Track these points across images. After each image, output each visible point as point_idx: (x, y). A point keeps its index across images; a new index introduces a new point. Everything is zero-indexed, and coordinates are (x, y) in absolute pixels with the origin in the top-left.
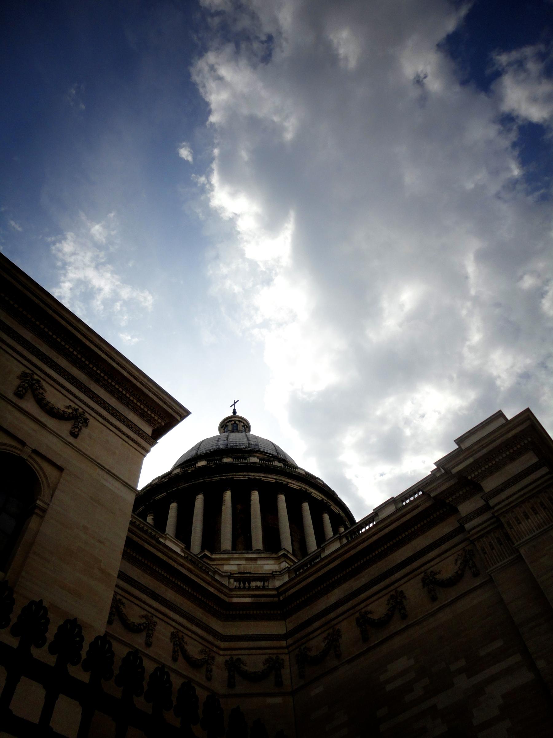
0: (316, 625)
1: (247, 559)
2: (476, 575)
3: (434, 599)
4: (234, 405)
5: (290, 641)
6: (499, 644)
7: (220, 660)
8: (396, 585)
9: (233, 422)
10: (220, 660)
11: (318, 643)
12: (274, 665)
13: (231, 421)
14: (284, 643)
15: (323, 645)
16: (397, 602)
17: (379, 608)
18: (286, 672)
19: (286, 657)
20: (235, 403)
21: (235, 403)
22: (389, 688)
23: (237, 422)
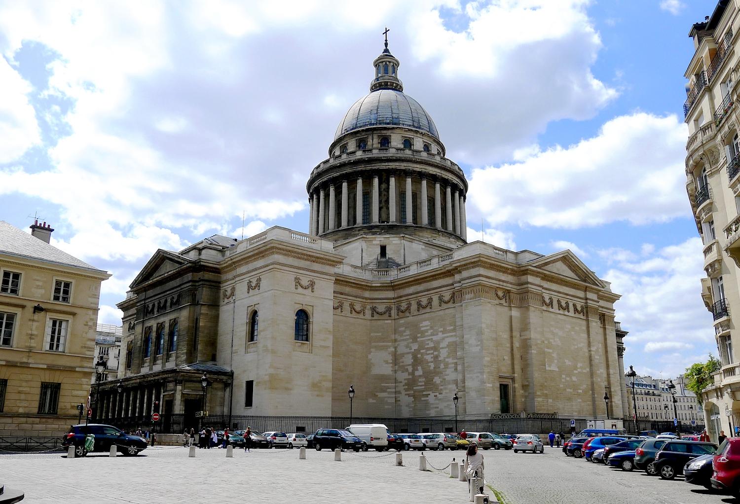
0: (404, 298)
1: (384, 238)
2: (454, 303)
4: (386, 33)
5: (395, 301)
6: (452, 327)
8: (431, 295)
9: (384, 63)
10: (368, 307)
11: (404, 306)
12: (389, 309)
13: (383, 62)
14: (393, 301)
16: (430, 301)
17: (424, 301)
19: (393, 306)
20: (386, 31)
21: (386, 31)
22: (422, 329)
23: (388, 63)
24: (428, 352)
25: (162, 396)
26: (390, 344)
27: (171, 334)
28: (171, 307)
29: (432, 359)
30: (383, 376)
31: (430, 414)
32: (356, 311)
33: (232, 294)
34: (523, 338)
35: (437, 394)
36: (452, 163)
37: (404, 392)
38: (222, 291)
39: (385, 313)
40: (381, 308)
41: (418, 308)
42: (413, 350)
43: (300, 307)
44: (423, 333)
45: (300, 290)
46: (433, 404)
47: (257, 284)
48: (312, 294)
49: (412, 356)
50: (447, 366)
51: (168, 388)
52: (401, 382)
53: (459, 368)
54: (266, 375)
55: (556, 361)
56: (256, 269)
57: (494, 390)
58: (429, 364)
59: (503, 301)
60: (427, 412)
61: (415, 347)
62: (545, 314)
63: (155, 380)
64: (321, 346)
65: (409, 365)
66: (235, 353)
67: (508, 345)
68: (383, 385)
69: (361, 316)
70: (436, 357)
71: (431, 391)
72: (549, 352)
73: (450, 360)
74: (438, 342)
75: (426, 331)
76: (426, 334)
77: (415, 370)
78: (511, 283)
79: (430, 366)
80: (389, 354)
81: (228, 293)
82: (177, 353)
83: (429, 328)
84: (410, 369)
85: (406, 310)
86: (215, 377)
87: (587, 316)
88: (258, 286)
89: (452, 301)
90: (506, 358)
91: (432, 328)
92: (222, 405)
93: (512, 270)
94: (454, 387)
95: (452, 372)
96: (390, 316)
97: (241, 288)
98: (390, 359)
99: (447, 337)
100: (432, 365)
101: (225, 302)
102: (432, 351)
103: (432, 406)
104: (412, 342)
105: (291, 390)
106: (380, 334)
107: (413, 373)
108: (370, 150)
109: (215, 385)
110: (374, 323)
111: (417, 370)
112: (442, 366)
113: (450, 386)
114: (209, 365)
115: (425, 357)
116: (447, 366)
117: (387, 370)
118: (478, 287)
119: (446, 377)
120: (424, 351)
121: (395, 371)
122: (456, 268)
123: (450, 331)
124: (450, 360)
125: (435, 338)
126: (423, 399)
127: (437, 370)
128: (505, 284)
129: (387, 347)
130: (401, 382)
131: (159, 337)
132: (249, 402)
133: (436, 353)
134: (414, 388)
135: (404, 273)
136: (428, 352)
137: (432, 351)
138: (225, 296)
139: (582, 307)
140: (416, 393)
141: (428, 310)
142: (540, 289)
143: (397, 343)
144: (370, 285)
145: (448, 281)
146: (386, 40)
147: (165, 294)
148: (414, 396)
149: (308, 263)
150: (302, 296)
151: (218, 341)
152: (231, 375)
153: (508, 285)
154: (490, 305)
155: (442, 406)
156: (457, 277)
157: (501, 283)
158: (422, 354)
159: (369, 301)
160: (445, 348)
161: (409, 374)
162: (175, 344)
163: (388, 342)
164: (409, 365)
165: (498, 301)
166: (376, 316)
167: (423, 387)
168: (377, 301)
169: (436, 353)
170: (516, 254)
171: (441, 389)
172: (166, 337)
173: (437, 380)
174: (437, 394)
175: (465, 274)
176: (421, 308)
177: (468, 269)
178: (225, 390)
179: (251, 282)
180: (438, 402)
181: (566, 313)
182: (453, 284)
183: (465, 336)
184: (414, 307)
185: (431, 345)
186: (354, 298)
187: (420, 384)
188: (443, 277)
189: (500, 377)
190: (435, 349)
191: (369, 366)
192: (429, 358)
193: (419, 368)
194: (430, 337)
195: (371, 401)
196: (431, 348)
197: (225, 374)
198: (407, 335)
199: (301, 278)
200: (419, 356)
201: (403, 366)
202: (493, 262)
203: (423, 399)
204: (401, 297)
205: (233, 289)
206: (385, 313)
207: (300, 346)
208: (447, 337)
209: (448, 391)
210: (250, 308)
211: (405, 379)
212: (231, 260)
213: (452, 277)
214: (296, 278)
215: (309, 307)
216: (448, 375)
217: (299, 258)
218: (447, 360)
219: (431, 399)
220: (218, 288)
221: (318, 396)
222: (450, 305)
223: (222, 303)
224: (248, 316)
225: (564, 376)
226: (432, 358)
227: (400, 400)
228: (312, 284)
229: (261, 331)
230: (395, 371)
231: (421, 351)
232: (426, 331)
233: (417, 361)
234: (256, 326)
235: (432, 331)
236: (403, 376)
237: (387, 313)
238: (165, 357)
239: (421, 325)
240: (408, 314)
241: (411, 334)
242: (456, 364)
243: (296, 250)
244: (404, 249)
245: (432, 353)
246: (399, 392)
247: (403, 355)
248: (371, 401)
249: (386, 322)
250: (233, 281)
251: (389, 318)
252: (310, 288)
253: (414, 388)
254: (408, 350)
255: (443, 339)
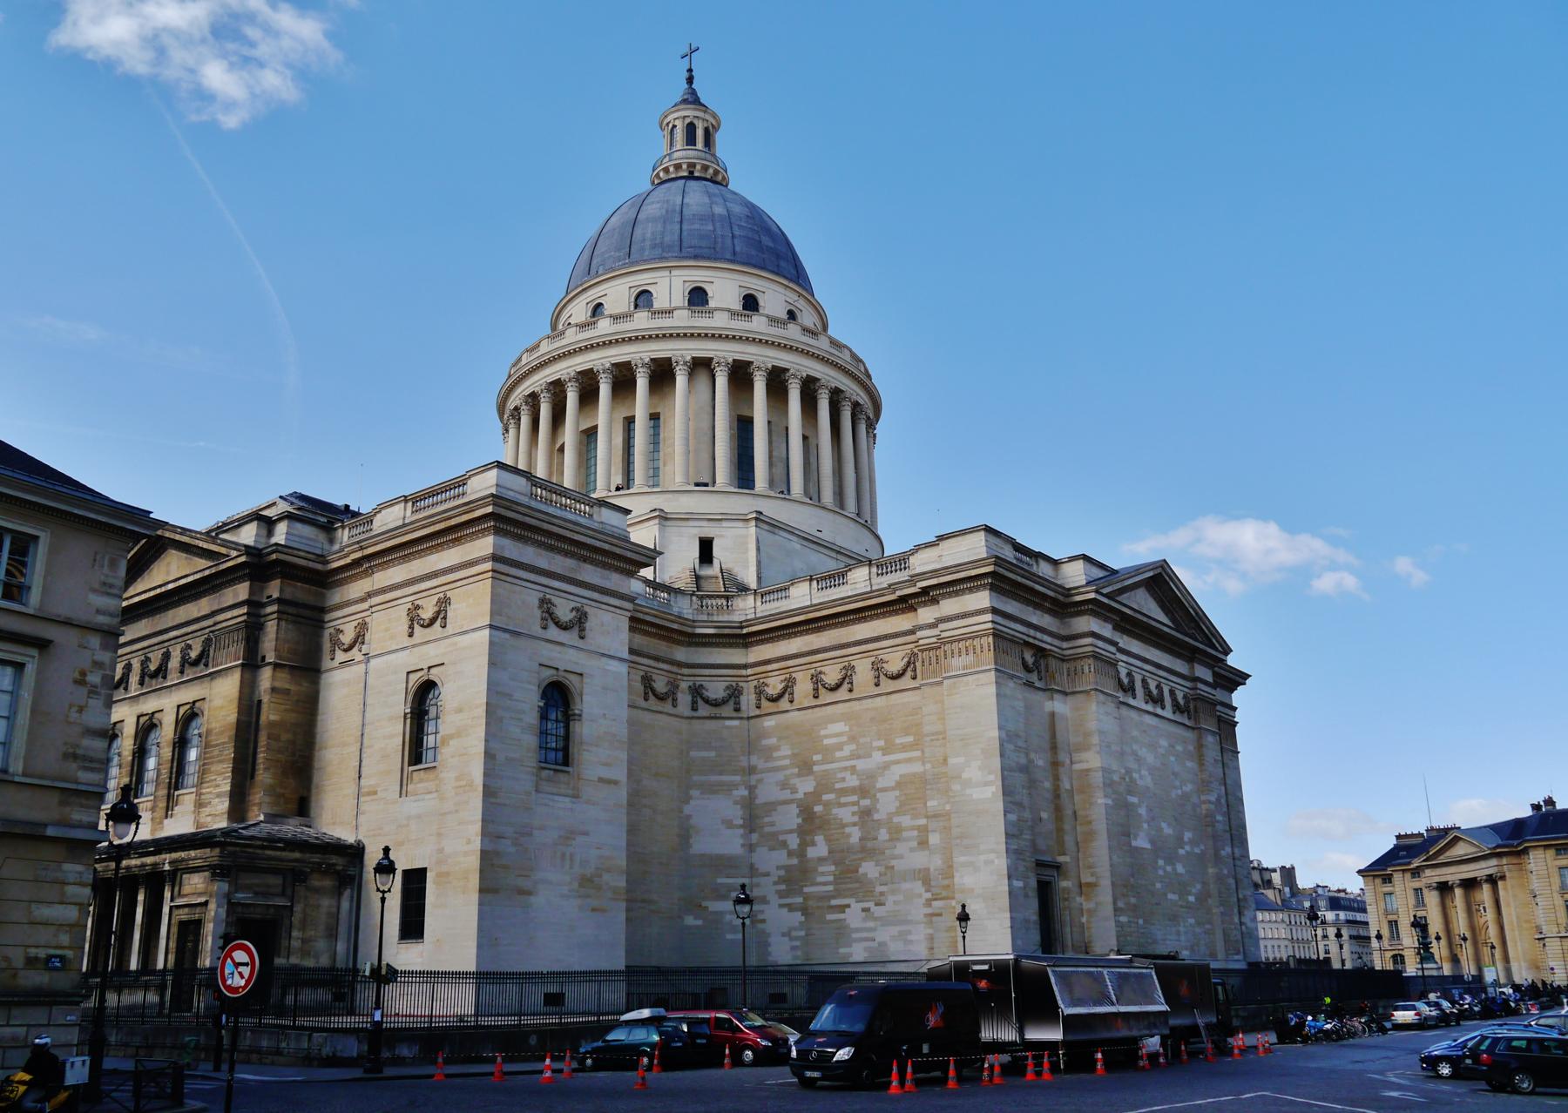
2: (914, 678)
3: (877, 685)
6: (910, 739)
7: (684, 685)
10: (684, 685)
15: (781, 686)
16: (847, 678)
17: (832, 675)
18: (743, 699)
22: (826, 742)
24: (843, 800)
25: (166, 910)
26: (737, 778)
27: (181, 744)
28: (182, 672)
29: (856, 819)
30: (720, 857)
31: (850, 955)
32: (656, 695)
33: (359, 639)
34: (1076, 767)
35: (871, 905)
36: (853, 356)
37: (775, 901)
38: (327, 633)
39: (724, 702)
40: (716, 690)
41: (816, 690)
42: (800, 795)
43: (548, 675)
44: (828, 752)
45: (553, 632)
46: (858, 930)
47: (438, 613)
48: (580, 643)
49: (797, 811)
50: (896, 833)
51: (186, 889)
52: (767, 874)
53: (934, 839)
54: (466, 854)
55: (1145, 826)
56: (383, 591)
57: (1026, 896)
58: (847, 830)
59: (1034, 677)
60: (842, 950)
61: (806, 786)
62: (1124, 711)
63: (143, 865)
64: (601, 780)
65: (791, 832)
66: (369, 794)
67: (1047, 785)
68: (719, 880)
69: (668, 707)
70: (866, 813)
71: (851, 896)
72: (1133, 804)
73: (906, 821)
74: (871, 776)
75: (840, 747)
76: (838, 754)
77: (804, 845)
78: (1050, 634)
79: (849, 835)
80: (736, 803)
81: (347, 638)
82: (199, 794)
83: (844, 739)
84: (794, 842)
85: (781, 696)
86: (316, 858)
87: (1197, 720)
88: (440, 616)
89: (909, 673)
90: (1044, 815)
91: (853, 739)
92: (332, 934)
93: (1054, 601)
94: (918, 887)
95: (912, 850)
96: (737, 710)
97: (387, 625)
98: (737, 814)
99: (898, 762)
100: (855, 835)
101: (336, 663)
102: (855, 798)
103: (854, 936)
104: (799, 775)
105: (529, 893)
106: (713, 754)
107: (801, 853)
108: (669, 312)
109: (316, 881)
110: (697, 724)
111: (813, 844)
112: (883, 835)
113: (906, 886)
114: (290, 828)
115: (835, 811)
116: (896, 833)
117: (731, 843)
118: (984, 640)
119: (893, 862)
120: (831, 796)
121: (751, 848)
122: (925, 591)
123: (905, 748)
124: (906, 821)
125: (861, 765)
126: (830, 917)
127: (869, 844)
128: (1039, 635)
129: (728, 788)
130: (767, 874)
131: (141, 753)
132: (412, 927)
133: (866, 802)
134: (806, 890)
135: (776, 604)
136: (843, 800)
137: (855, 798)
138: (336, 643)
139: (1185, 697)
140: (810, 903)
141: (842, 694)
142: (1112, 649)
143: (753, 779)
144: (689, 630)
145: (900, 622)
146: (690, 70)
147: (165, 637)
148: (805, 910)
149: (570, 562)
150: (558, 648)
151: (316, 765)
152: (355, 852)
153: (1046, 638)
154: (1011, 684)
155: (884, 935)
156: (926, 614)
157: (1032, 632)
158: (827, 804)
159: (686, 671)
160: (893, 789)
161: (790, 854)
162: (191, 769)
163: (735, 772)
164: (791, 832)
165: (1022, 674)
166: (704, 710)
167: (831, 888)
168: (707, 672)
169: (866, 802)
170: (1055, 563)
171: (882, 894)
172: (167, 752)
173: (869, 869)
174: (871, 905)
175: (949, 606)
176: (822, 691)
177: (957, 593)
178: (340, 894)
179: (418, 607)
180: (871, 924)
181: (1159, 711)
182: (912, 632)
183: (952, 761)
184: (803, 687)
185: (853, 781)
186: (651, 662)
187: (820, 879)
188: (884, 615)
189: (1040, 864)
190: (863, 791)
191: (685, 834)
192: (846, 814)
193: (819, 839)
194: (852, 763)
195: (690, 921)
196: (853, 791)
197: (338, 848)
198: (785, 757)
199: (554, 599)
200: (818, 809)
201: (774, 835)
202: (1019, 579)
203: (830, 917)
204: (768, 662)
205: (362, 629)
206: (724, 702)
207: (549, 780)
208: (898, 762)
209: (901, 897)
210: (414, 677)
211: (778, 868)
212: (362, 548)
213: (911, 615)
214: (543, 601)
215: (572, 677)
216: (901, 857)
217: (551, 548)
218: (895, 820)
219: (853, 916)
220: (319, 625)
221: (593, 910)
222: (906, 682)
223: (326, 663)
224: (410, 698)
225: (1161, 862)
226: (854, 814)
227: (763, 921)
228: (580, 620)
229: (451, 737)
230: (751, 848)
231: (825, 797)
232: (840, 747)
233: (811, 822)
234: (431, 728)
235: (854, 747)
236: (772, 861)
237: (731, 702)
238: (162, 804)
239: (823, 733)
240: (784, 704)
241: (794, 755)
242: (924, 830)
243: (546, 526)
244: (758, 549)
245: (854, 804)
246: (764, 900)
247: (771, 807)
248: (690, 921)
249: (728, 723)
250: (365, 605)
251: (735, 714)
252: (576, 629)
253: (806, 890)
254: (786, 795)
255: (886, 766)
